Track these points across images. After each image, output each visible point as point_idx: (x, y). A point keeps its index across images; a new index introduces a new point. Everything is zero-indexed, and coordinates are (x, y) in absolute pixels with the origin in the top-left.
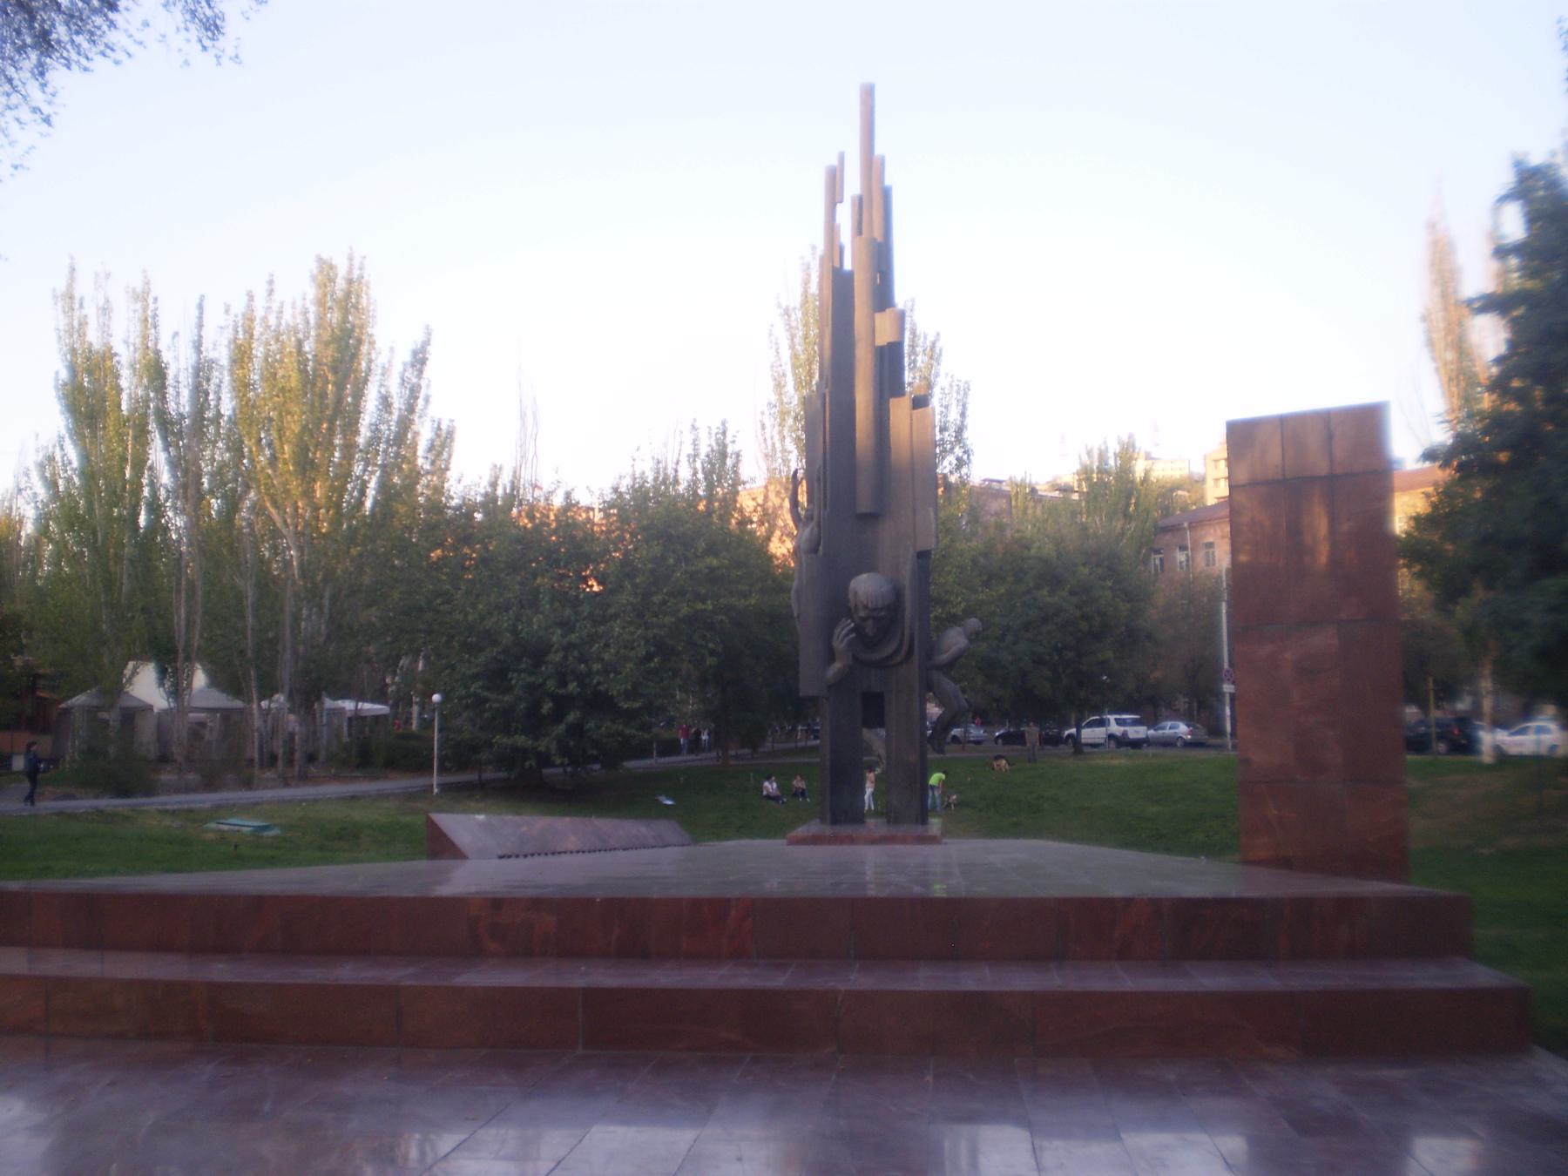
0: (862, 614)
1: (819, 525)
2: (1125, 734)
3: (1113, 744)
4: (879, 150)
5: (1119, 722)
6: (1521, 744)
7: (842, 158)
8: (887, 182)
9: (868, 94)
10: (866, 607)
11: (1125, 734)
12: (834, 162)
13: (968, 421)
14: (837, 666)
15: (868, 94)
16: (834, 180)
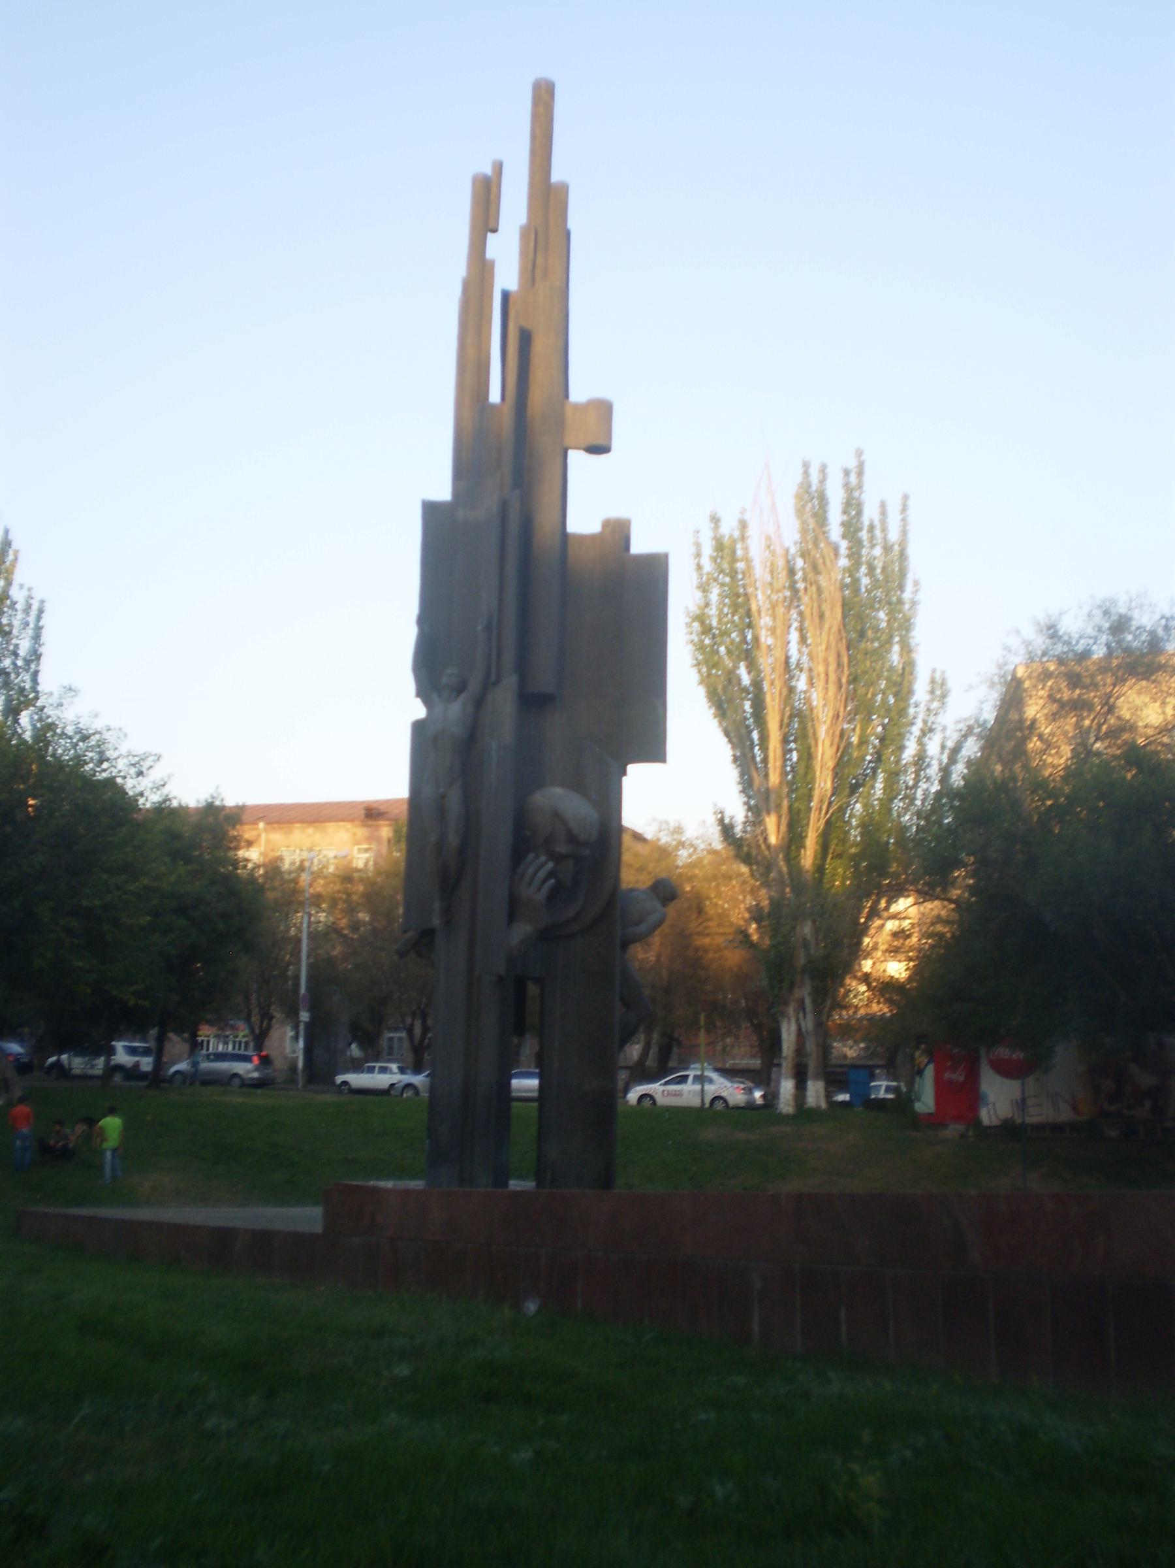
0: (562, 848)
1: (479, 703)
2: (137, 1065)
3: (118, 1078)
4: (555, 177)
5: (132, 1051)
6: (678, 1094)
7: (498, 167)
8: (571, 225)
9: (544, 97)
10: (572, 838)
11: (137, 1065)
12: (488, 171)
13: (42, 650)
14: (522, 930)
15: (544, 97)
16: (486, 195)
